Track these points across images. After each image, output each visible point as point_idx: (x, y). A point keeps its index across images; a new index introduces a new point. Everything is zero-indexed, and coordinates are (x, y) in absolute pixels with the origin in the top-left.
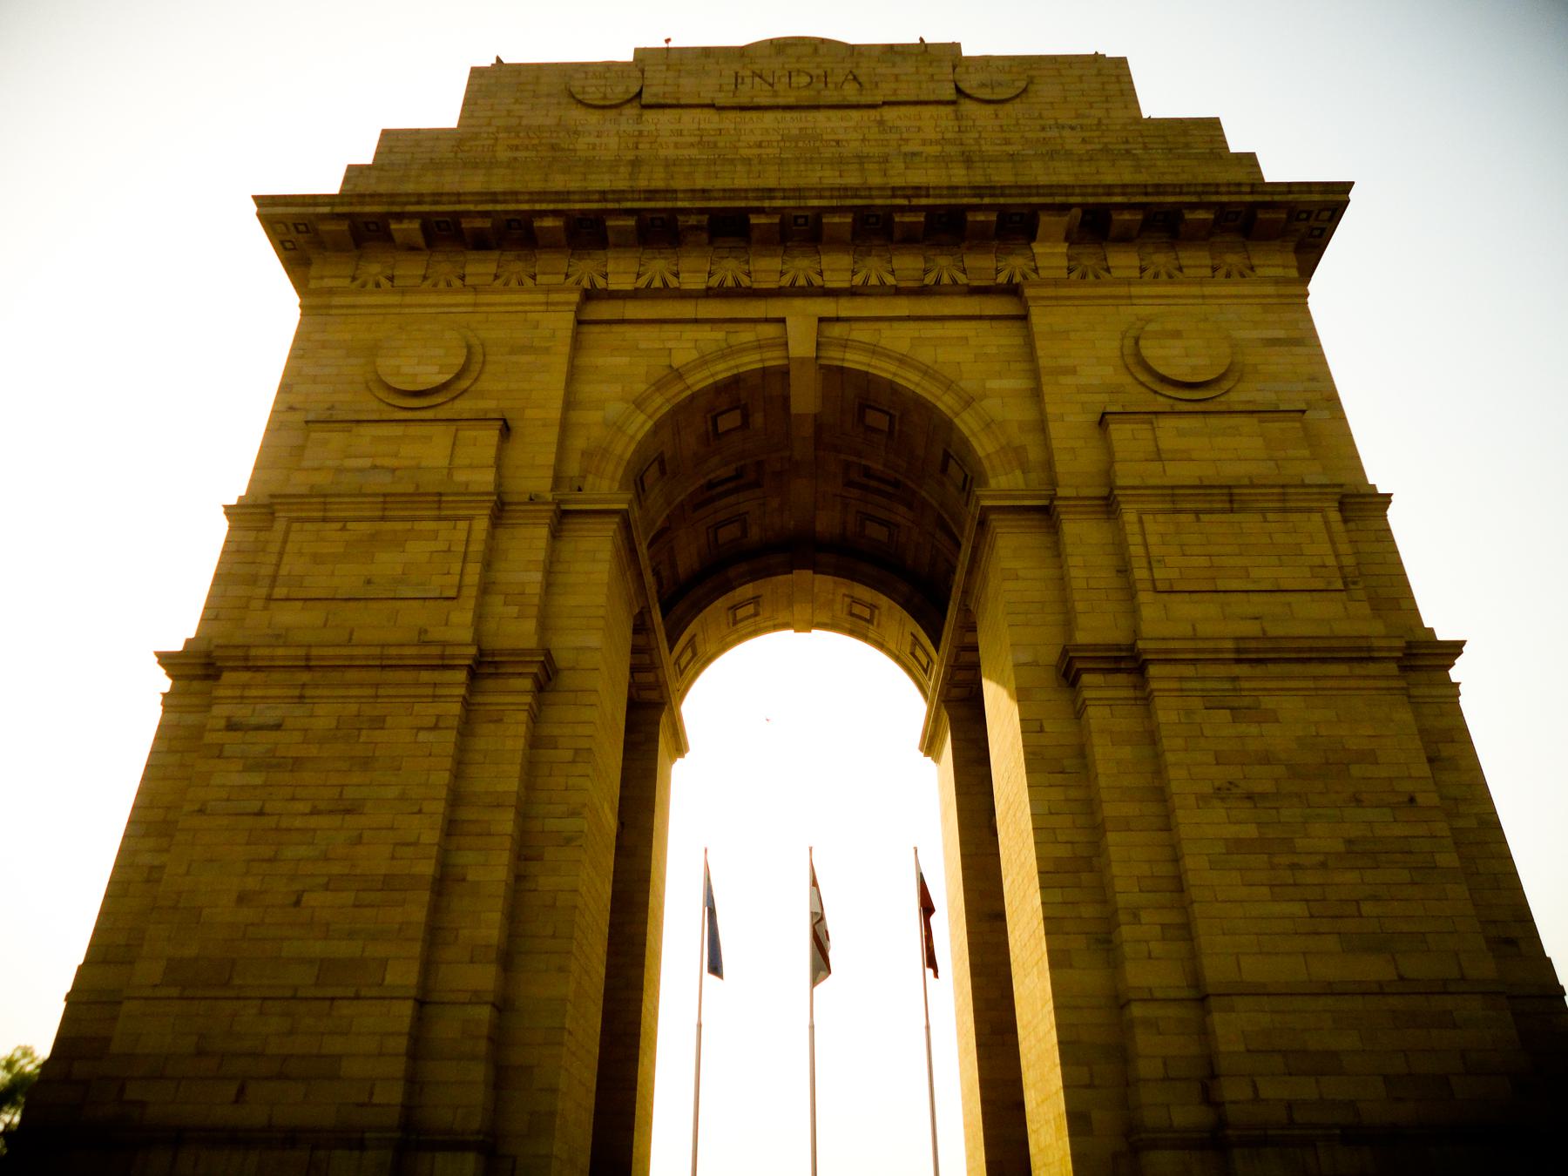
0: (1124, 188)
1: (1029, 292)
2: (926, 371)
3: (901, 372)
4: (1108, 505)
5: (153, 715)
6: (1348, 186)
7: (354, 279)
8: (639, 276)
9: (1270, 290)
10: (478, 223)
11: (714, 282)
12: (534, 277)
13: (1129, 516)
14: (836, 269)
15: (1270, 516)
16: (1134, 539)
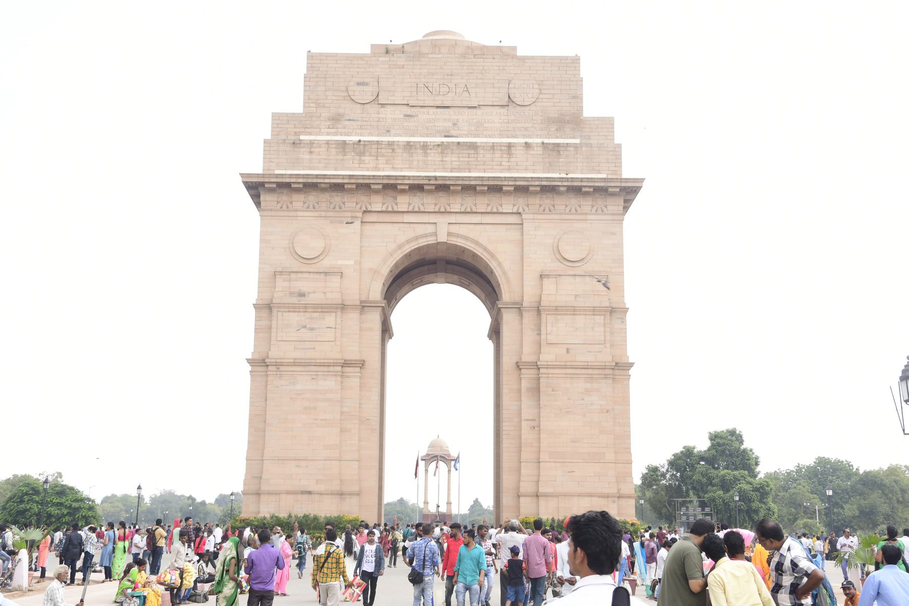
0: (561, 180)
1: (524, 216)
2: (485, 249)
3: (477, 248)
4: (539, 311)
5: (248, 377)
6: (642, 180)
7: (278, 202)
8: (383, 204)
9: (610, 217)
10: (323, 186)
11: (410, 209)
12: (344, 203)
13: (543, 316)
14: (457, 203)
15: (588, 317)
16: (543, 325)
